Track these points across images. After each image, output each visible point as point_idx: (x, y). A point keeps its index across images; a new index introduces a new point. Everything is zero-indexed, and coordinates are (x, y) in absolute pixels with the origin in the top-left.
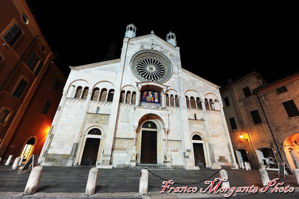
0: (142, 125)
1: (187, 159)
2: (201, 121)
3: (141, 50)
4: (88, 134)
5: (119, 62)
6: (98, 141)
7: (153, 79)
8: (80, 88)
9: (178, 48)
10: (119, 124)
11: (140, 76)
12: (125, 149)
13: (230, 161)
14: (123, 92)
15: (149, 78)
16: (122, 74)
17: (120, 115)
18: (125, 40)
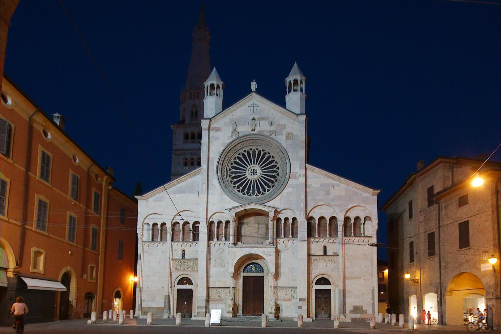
0: (242, 269)
1: (300, 309)
2: (333, 257)
3: (234, 138)
4: (178, 284)
5: (199, 173)
6: (189, 293)
7: (256, 192)
8: (155, 225)
9: (303, 118)
10: (213, 270)
11: (236, 190)
12: (222, 300)
13: (370, 312)
14: (210, 224)
15: (251, 191)
16: (206, 195)
17: (211, 257)
18: (204, 124)
